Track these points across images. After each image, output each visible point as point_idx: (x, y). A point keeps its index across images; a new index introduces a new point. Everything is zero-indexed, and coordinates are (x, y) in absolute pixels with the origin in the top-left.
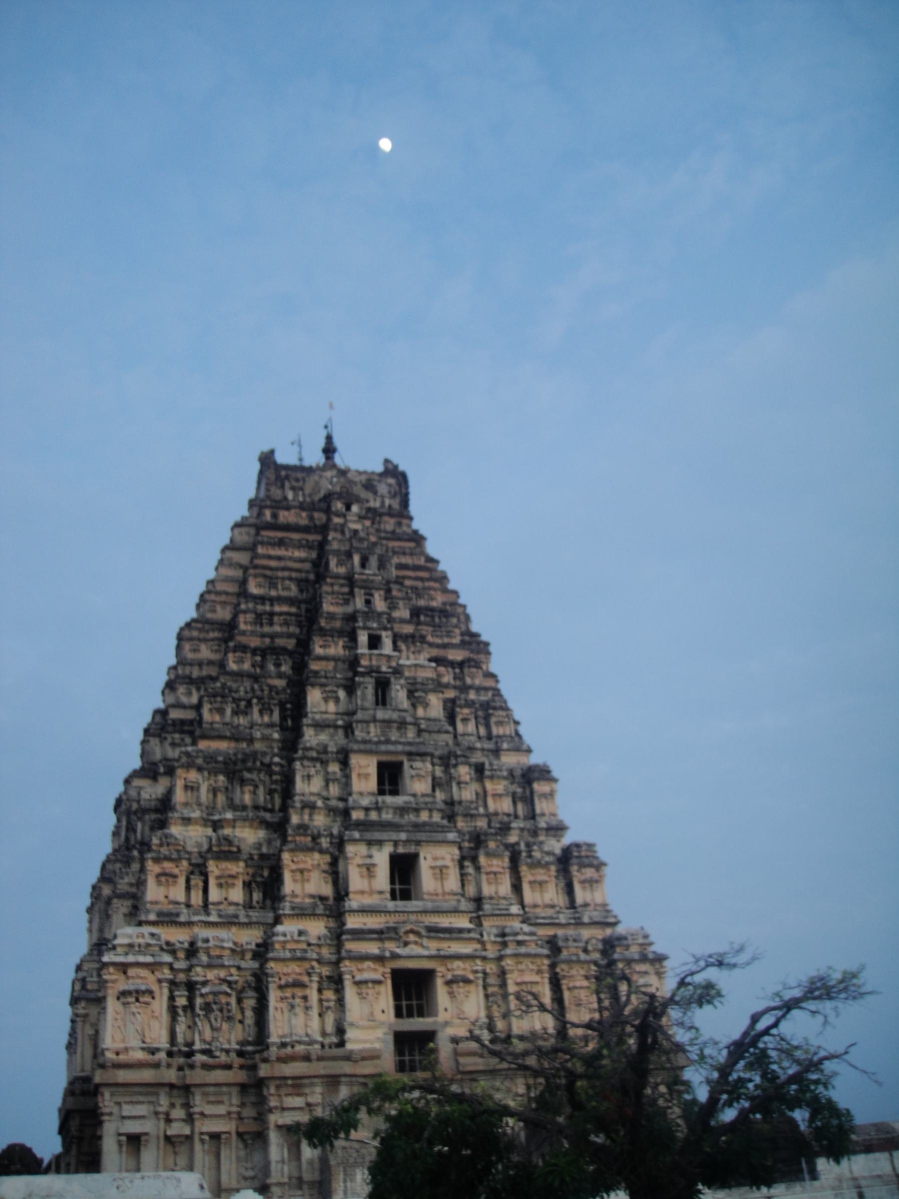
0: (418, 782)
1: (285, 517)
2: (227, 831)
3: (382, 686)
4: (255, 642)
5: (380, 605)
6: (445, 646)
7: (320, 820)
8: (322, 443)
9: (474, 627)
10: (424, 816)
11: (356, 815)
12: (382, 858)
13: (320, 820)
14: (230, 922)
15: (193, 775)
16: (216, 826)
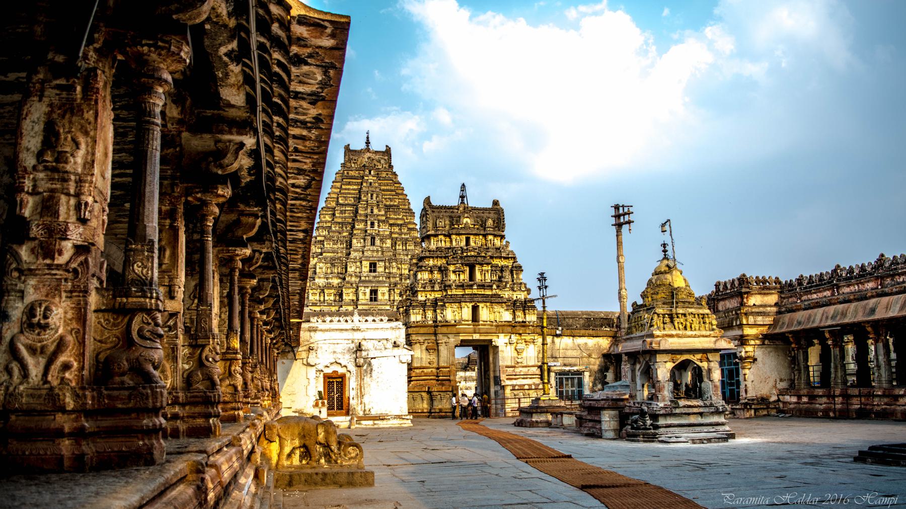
0: (380, 269)
1: (352, 173)
2: (330, 280)
3: (373, 239)
4: (340, 220)
5: (376, 211)
6: (397, 219)
7: (353, 279)
8: (365, 141)
9: (412, 207)
10: (381, 279)
11: (363, 278)
12: (368, 291)
13: (353, 279)
14: (330, 305)
15: (321, 265)
16: (327, 279)
